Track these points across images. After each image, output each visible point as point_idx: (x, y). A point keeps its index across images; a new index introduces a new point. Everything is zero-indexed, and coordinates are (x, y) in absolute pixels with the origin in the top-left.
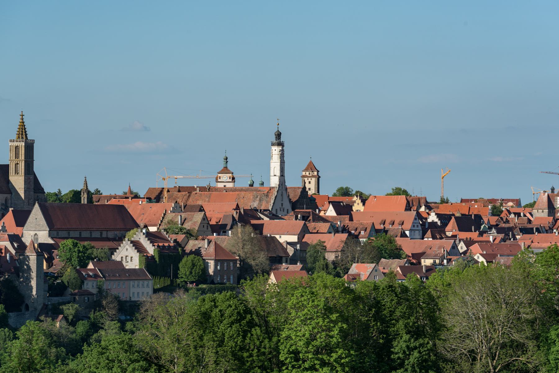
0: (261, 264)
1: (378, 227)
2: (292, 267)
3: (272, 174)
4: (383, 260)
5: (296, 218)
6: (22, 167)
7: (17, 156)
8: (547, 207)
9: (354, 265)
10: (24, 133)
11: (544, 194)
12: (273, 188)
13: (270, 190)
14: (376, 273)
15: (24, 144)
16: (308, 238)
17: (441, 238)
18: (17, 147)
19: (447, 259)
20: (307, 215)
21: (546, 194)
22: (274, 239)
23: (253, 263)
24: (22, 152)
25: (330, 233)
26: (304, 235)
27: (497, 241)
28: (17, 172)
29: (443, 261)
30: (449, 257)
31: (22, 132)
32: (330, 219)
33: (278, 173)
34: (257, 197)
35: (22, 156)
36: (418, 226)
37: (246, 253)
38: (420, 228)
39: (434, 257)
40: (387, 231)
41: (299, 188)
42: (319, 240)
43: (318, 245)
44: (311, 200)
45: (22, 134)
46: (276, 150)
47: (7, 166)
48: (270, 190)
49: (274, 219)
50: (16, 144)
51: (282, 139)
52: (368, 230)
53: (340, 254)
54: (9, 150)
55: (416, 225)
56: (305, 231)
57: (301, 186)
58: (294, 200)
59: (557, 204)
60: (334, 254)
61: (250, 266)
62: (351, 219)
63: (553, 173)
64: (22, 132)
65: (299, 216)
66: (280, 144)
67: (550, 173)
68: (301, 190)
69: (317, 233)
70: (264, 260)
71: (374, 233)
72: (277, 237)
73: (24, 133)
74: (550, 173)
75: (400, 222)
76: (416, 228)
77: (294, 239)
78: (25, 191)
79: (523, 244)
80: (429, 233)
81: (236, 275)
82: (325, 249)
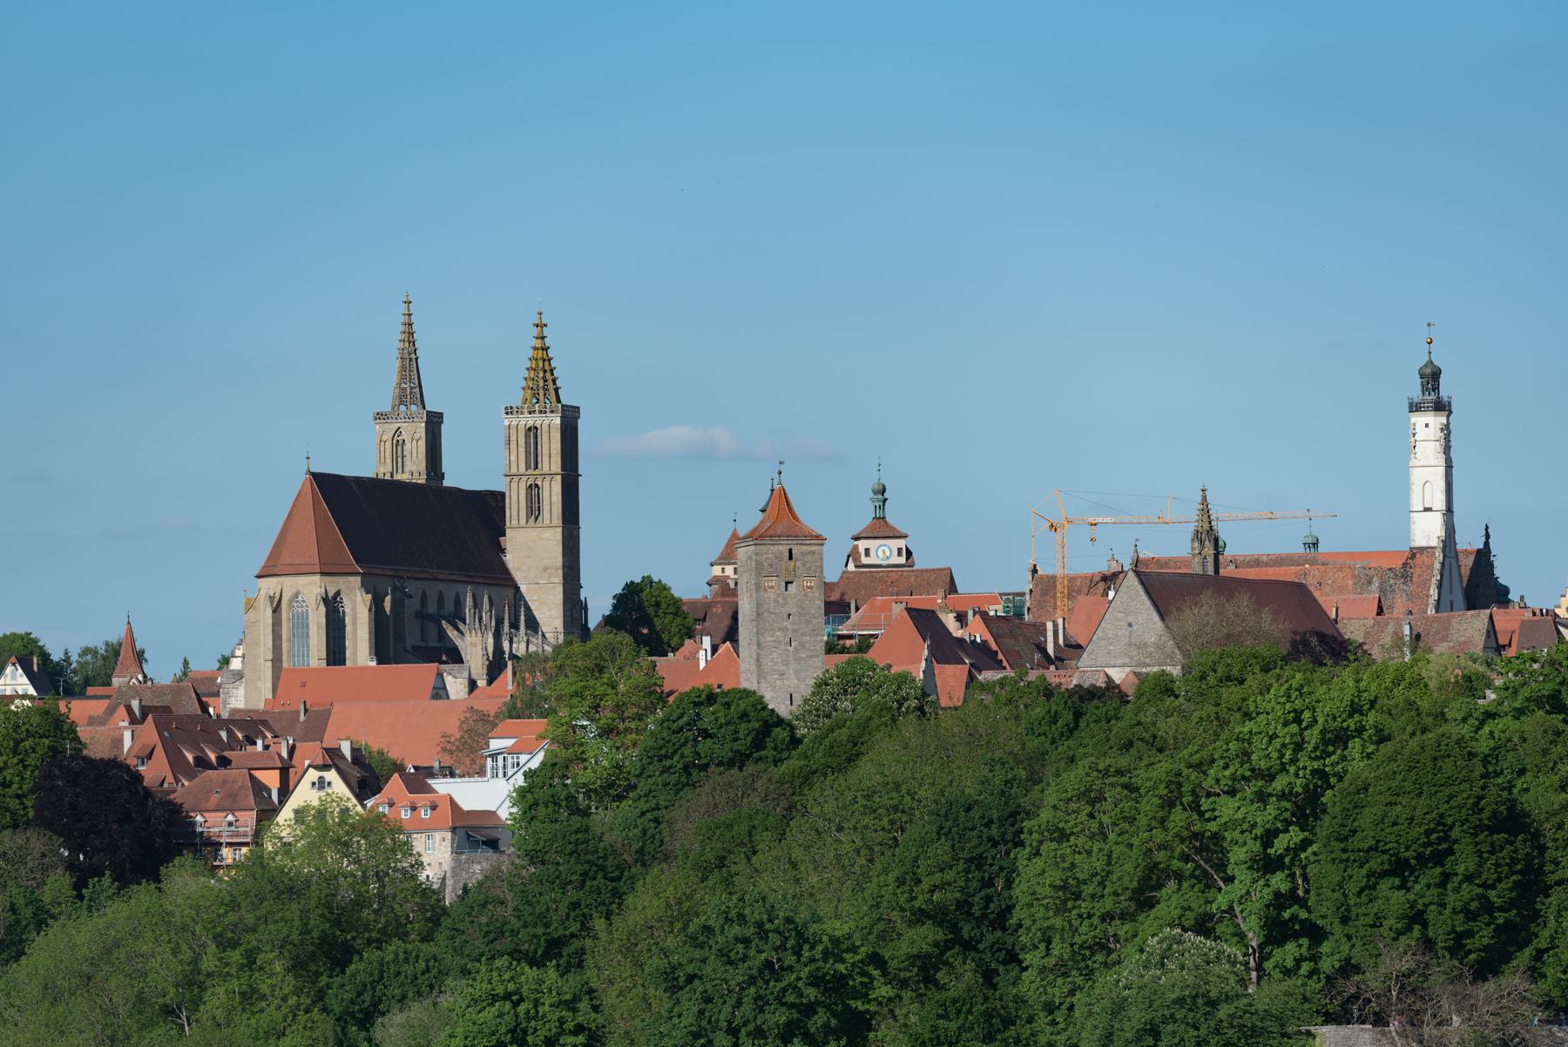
3: (1417, 504)
6: (552, 493)
7: (533, 459)
10: (551, 386)
12: (1422, 549)
13: (1413, 556)
15: (558, 421)
18: (532, 431)
24: (552, 447)
28: (534, 510)
31: (543, 379)
33: (1439, 503)
34: (1370, 582)
35: (552, 459)
45: (546, 390)
46: (1427, 426)
47: (499, 497)
48: (1413, 556)
50: (527, 420)
51: (1445, 391)
54: (503, 440)
64: (543, 379)
66: (1441, 406)
73: (551, 386)
78: (565, 576)
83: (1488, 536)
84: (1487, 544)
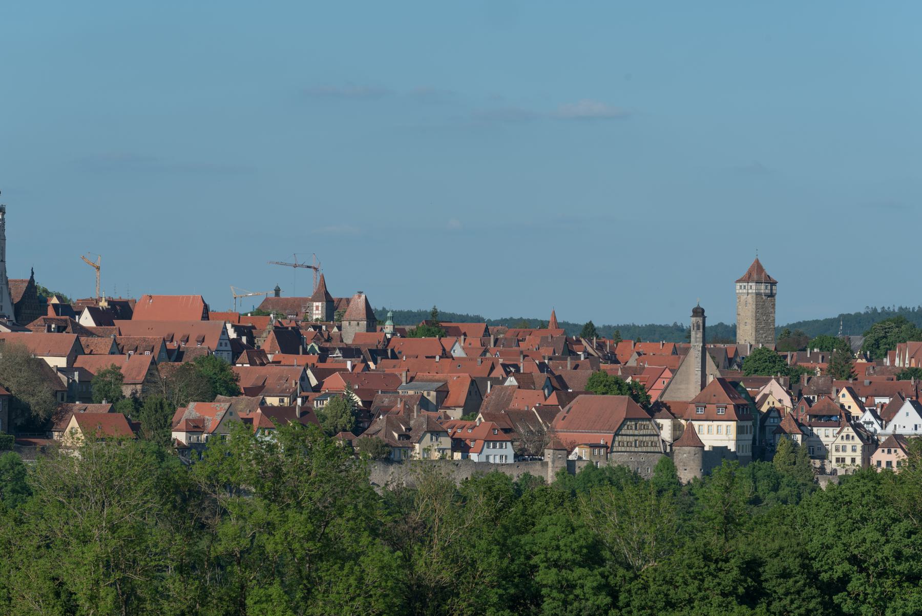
0: (45, 402)
1: (169, 346)
2: (92, 407)
4: (219, 397)
5: (49, 330)
8: (364, 316)
9: (192, 405)
11: (360, 296)
14: (228, 417)
16: (80, 361)
17: (262, 364)
19: (303, 398)
20: (64, 325)
21: (363, 296)
22: (42, 364)
23: (32, 401)
25: (113, 353)
26: (76, 357)
27: (356, 371)
29: (295, 400)
30: (304, 394)
32: (94, 331)
36: (226, 344)
37: (19, 383)
38: (229, 348)
39: (280, 394)
40: (183, 352)
41: (22, 281)
42: (113, 365)
43: (109, 372)
44: (40, 302)
49: (17, 331)
52: (157, 350)
53: (139, 387)
55: (223, 342)
56: (77, 351)
57: (29, 278)
58: (17, 300)
59: (312, 314)
60: (133, 386)
61: (26, 408)
62: (120, 334)
63: (286, 264)
65: (53, 326)
67: (282, 264)
68: (26, 284)
69: (90, 354)
70: (49, 395)
71: (164, 355)
72: (45, 358)
74: (282, 264)
75: (199, 337)
76: (223, 348)
77: (62, 362)
79: (404, 374)
80: (244, 354)
81: (6, 422)
82: (120, 378)
83: (33, 273)
84: (32, 277)
